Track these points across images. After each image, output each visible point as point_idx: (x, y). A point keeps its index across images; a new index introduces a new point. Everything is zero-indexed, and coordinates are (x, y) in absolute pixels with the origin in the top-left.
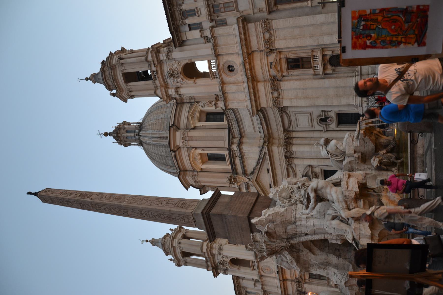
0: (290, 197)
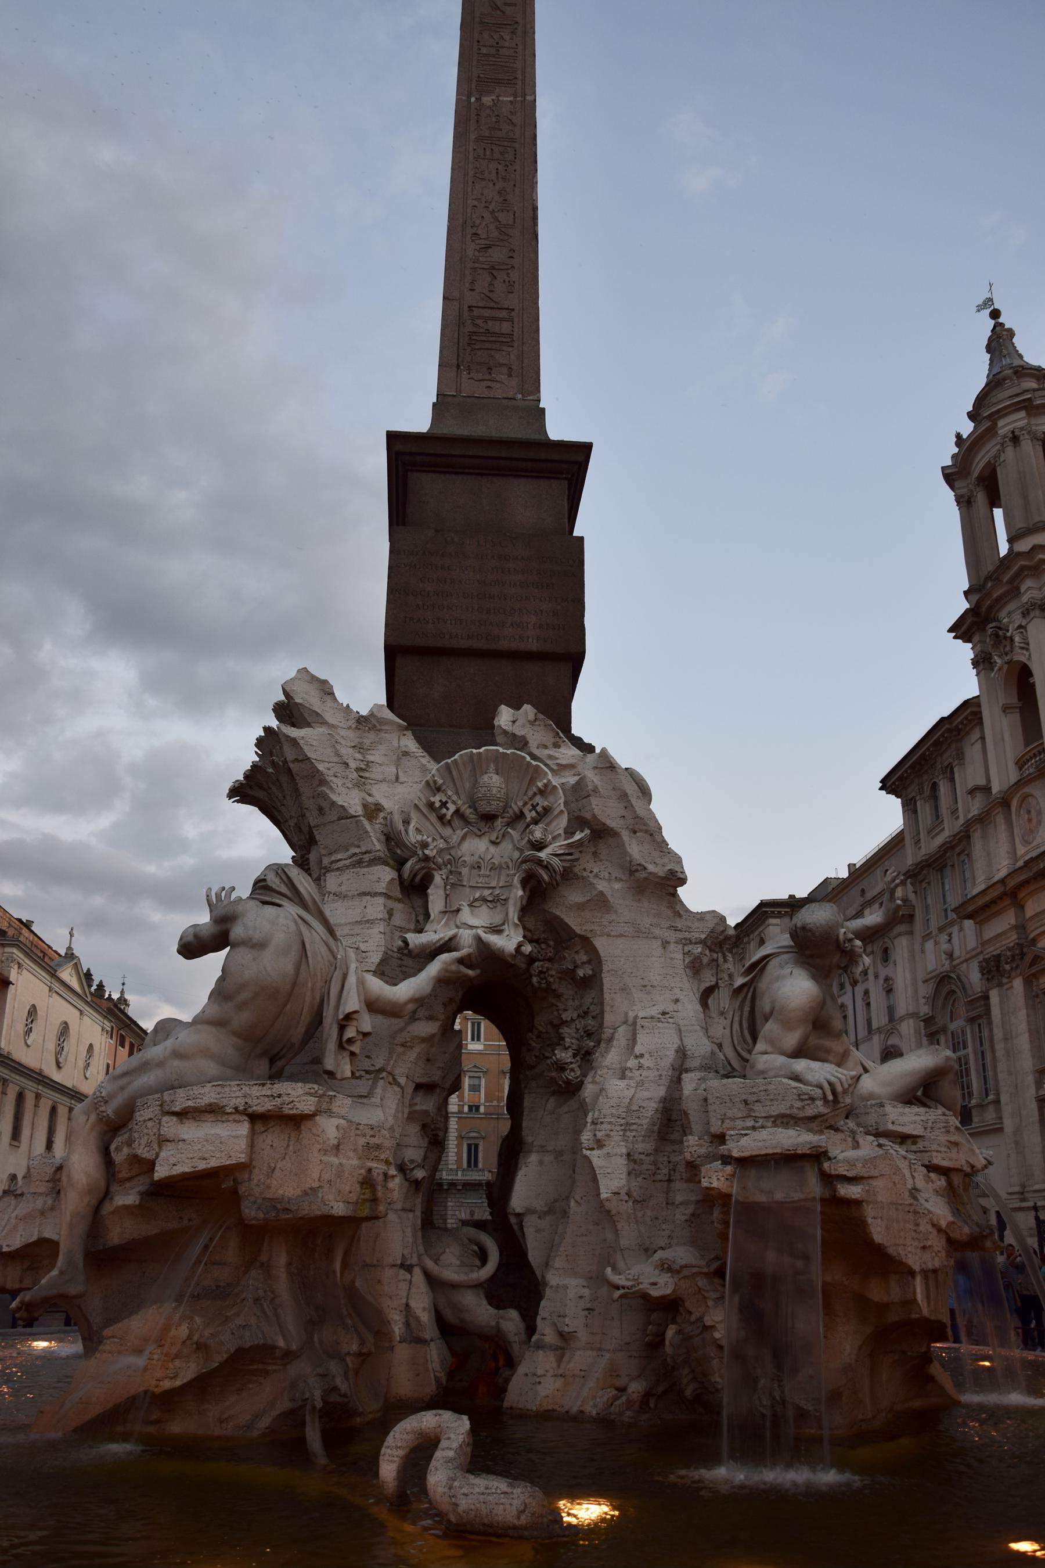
0: (489, 818)
